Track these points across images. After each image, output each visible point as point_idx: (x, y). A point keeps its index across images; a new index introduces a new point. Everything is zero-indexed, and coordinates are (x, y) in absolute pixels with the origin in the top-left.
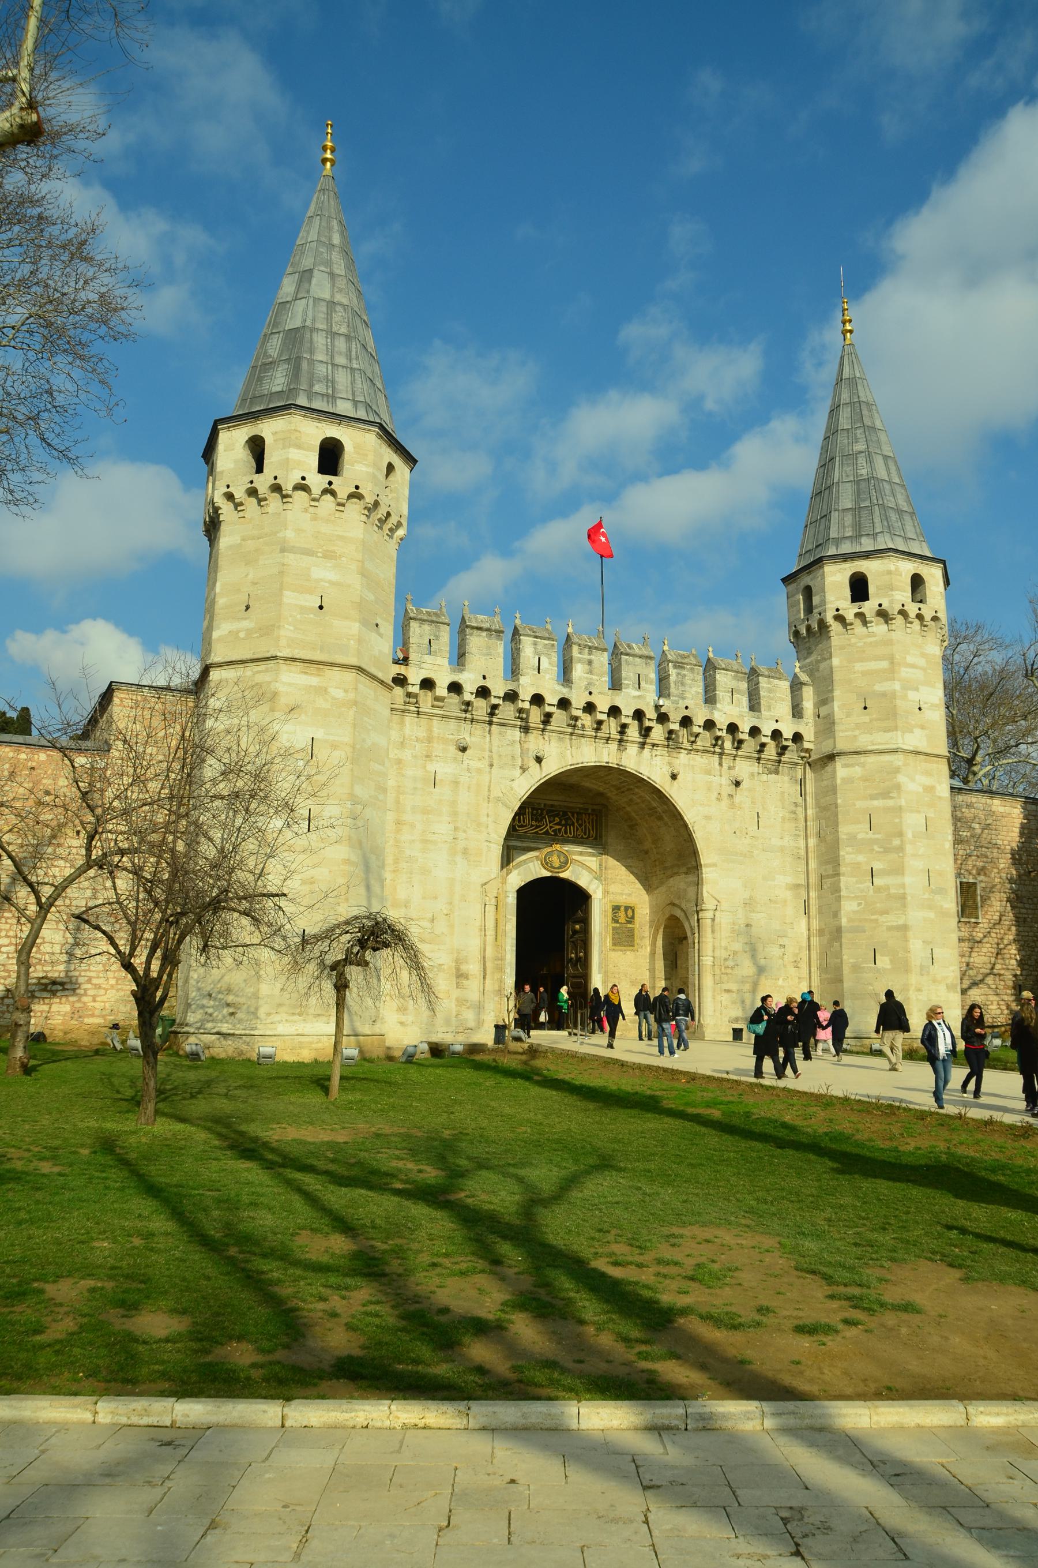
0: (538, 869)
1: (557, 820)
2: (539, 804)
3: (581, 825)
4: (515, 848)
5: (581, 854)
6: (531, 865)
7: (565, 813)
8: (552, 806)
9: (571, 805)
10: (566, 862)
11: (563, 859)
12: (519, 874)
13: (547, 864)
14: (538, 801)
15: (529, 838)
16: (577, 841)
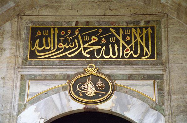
0: (65, 101)
1: (94, 39)
2: (69, 22)
3: (129, 43)
4: (33, 78)
5: (130, 77)
6: (55, 97)
7: (106, 30)
8: (87, 23)
9: (114, 19)
10: (107, 89)
11: (100, 85)
12: (36, 110)
13: (77, 93)
14: (67, 19)
15: (53, 64)
16: (121, 61)
